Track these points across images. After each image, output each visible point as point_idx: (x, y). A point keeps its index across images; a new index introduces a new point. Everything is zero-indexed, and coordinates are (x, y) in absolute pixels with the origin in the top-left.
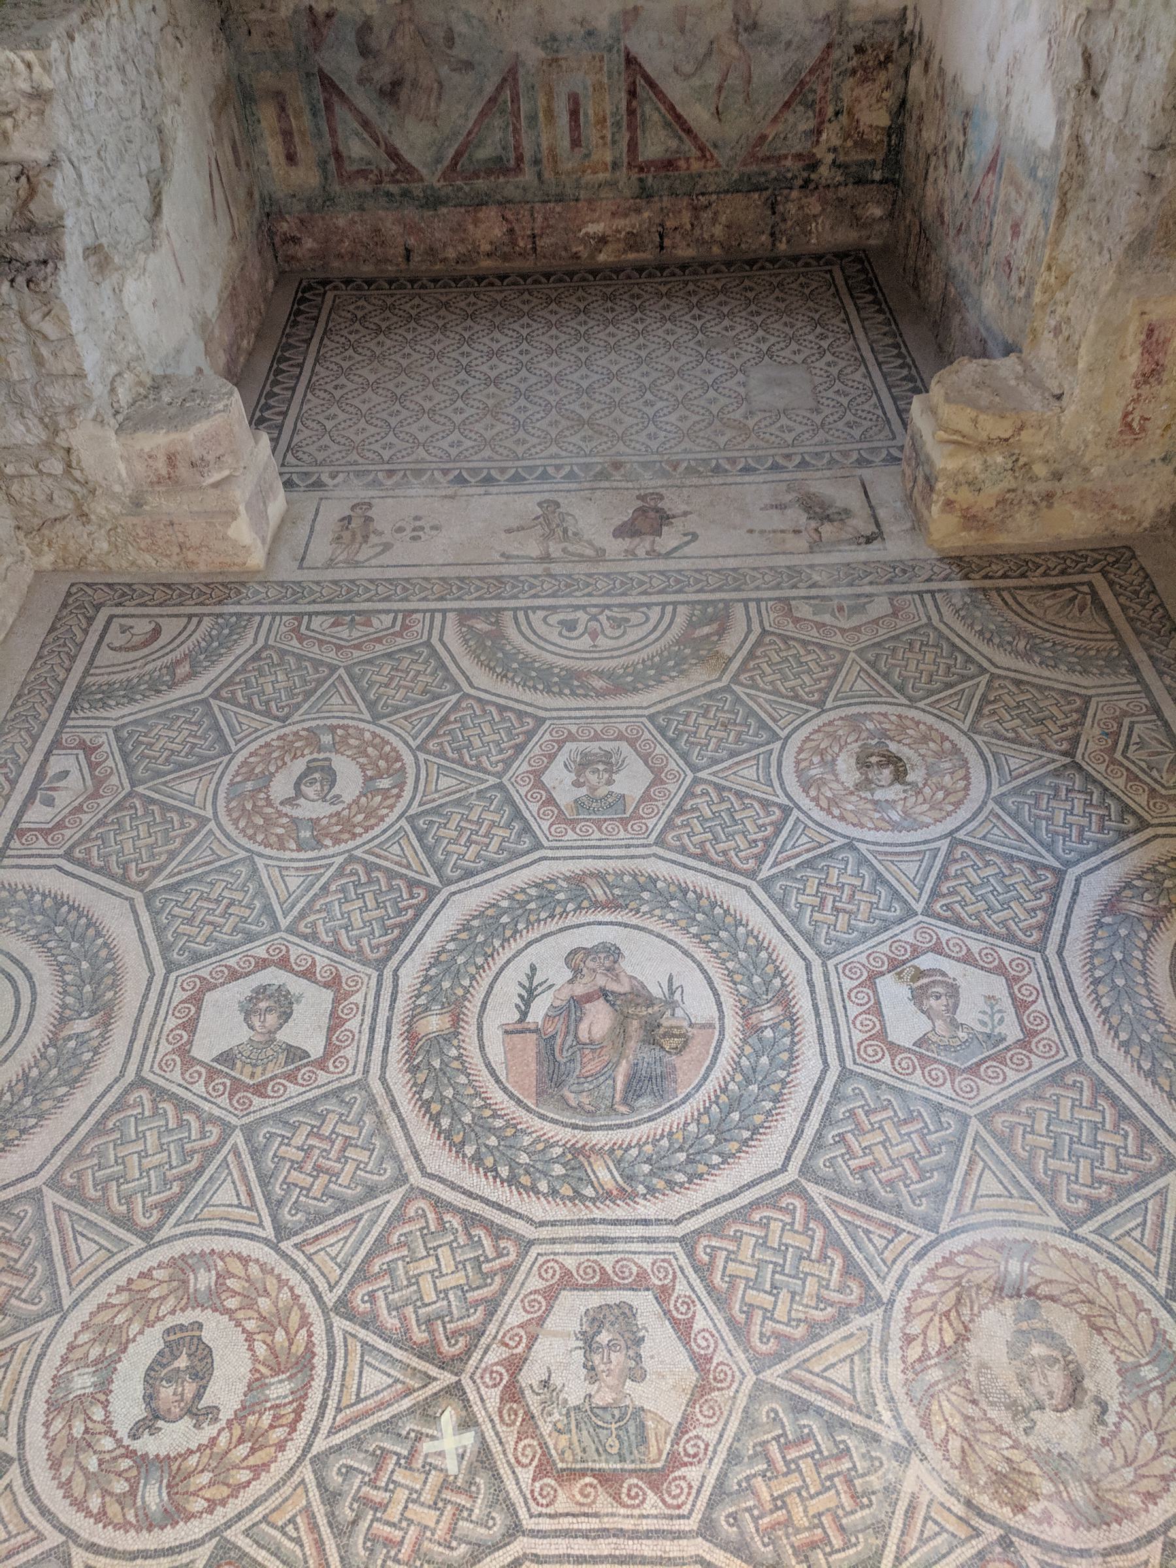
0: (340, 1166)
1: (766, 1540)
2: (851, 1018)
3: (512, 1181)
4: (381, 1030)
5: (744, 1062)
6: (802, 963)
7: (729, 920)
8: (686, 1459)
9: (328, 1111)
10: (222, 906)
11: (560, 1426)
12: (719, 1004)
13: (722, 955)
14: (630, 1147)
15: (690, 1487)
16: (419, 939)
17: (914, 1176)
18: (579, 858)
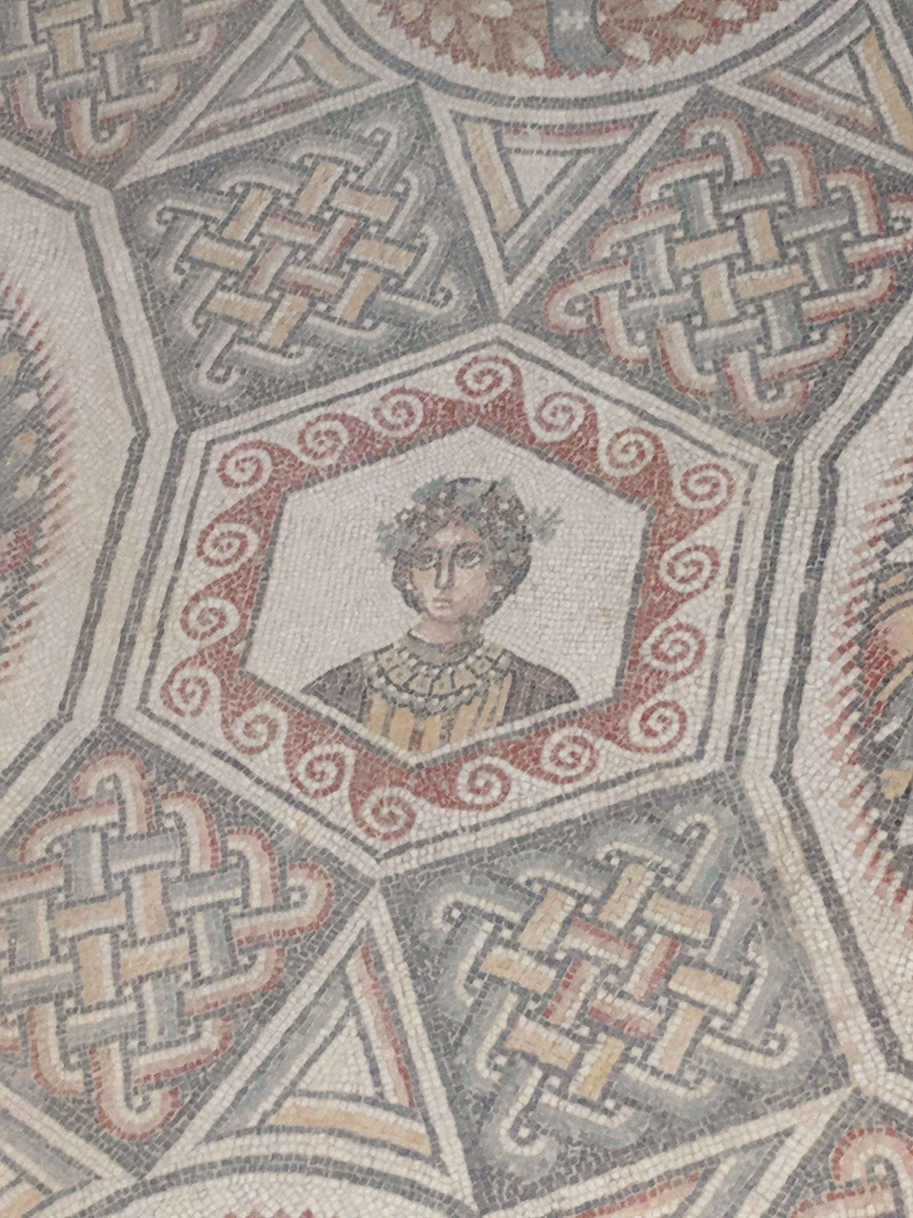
0: (655, 1017)
9: (626, 859)
10: (332, 240)
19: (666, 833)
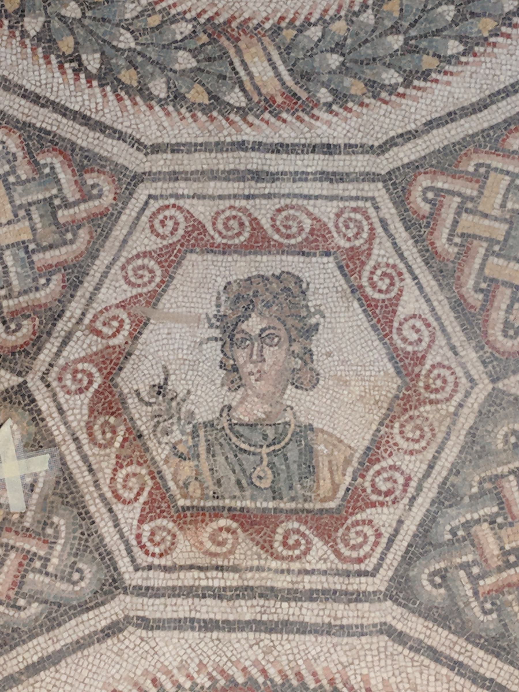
1: (488, 606)
8: (374, 497)
11: (181, 448)
14: (308, 23)
15: (379, 535)
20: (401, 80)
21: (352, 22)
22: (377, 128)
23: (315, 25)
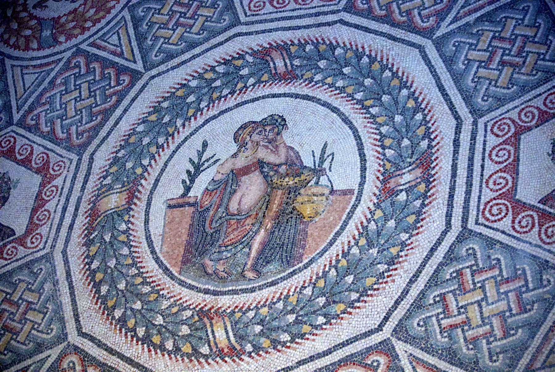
2: (486, 177)
3: (146, 340)
4: (71, 209)
5: (372, 226)
6: (454, 122)
7: (396, 82)
12: (363, 169)
13: (379, 120)
14: (249, 309)
16: (117, 123)
17: (498, 333)
18: (270, 31)
19: (32, 272)
20: (289, 339)
21: (271, 308)
22: (272, 365)
23: (252, 310)
